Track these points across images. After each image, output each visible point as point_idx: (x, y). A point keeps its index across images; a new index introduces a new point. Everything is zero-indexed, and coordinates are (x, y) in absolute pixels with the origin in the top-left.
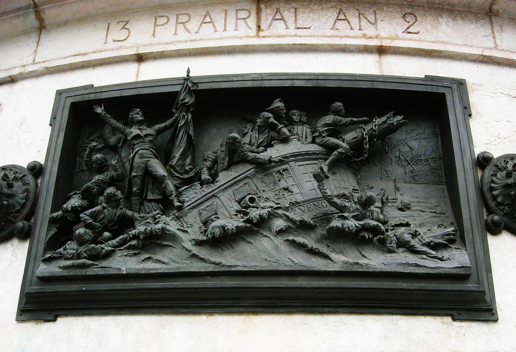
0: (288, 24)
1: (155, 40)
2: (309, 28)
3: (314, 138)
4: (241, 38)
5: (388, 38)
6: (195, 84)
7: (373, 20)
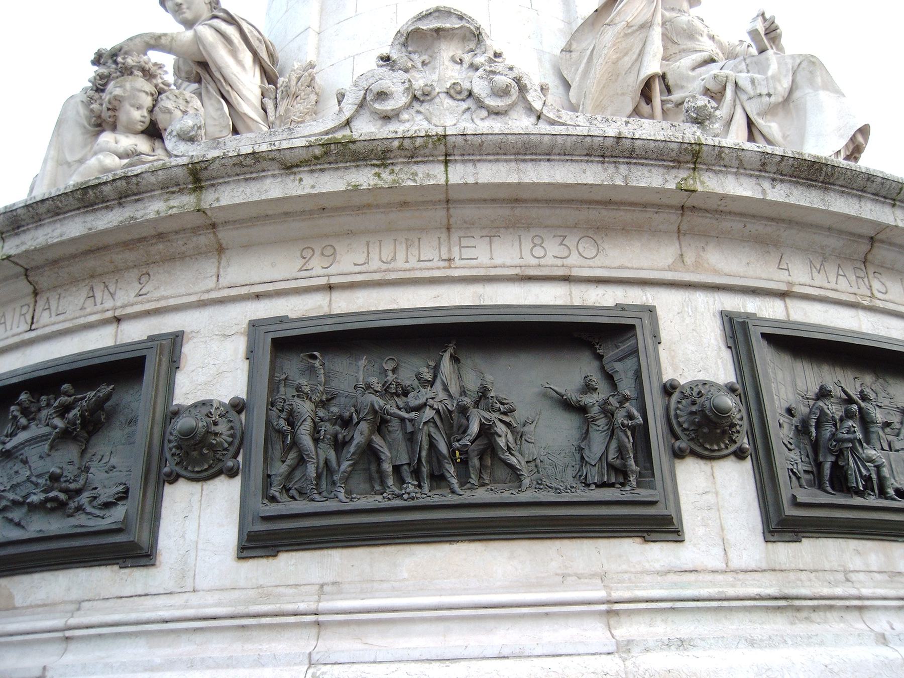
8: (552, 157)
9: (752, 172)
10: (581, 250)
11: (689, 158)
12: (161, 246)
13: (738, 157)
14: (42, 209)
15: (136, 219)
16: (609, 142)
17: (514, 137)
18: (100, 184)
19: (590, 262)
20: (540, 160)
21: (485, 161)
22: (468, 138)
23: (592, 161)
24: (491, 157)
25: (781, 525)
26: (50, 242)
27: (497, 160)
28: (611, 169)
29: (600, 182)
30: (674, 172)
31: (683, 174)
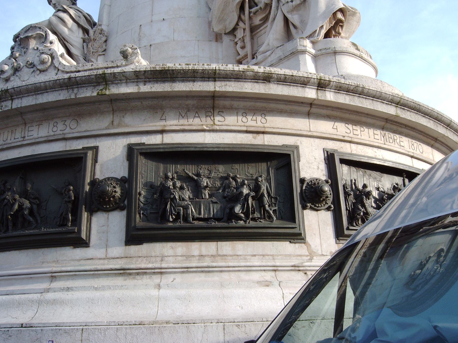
8: (48, 91)
9: (133, 80)
10: (71, 125)
11: (102, 80)
13: (123, 76)
16: (66, 81)
17: (31, 86)
19: (73, 131)
20: (44, 93)
21: (25, 96)
22: (15, 89)
23: (63, 89)
24: (26, 95)
25: (134, 237)
27: (29, 96)
28: (71, 91)
29: (65, 98)
30: (97, 87)
31: (101, 87)
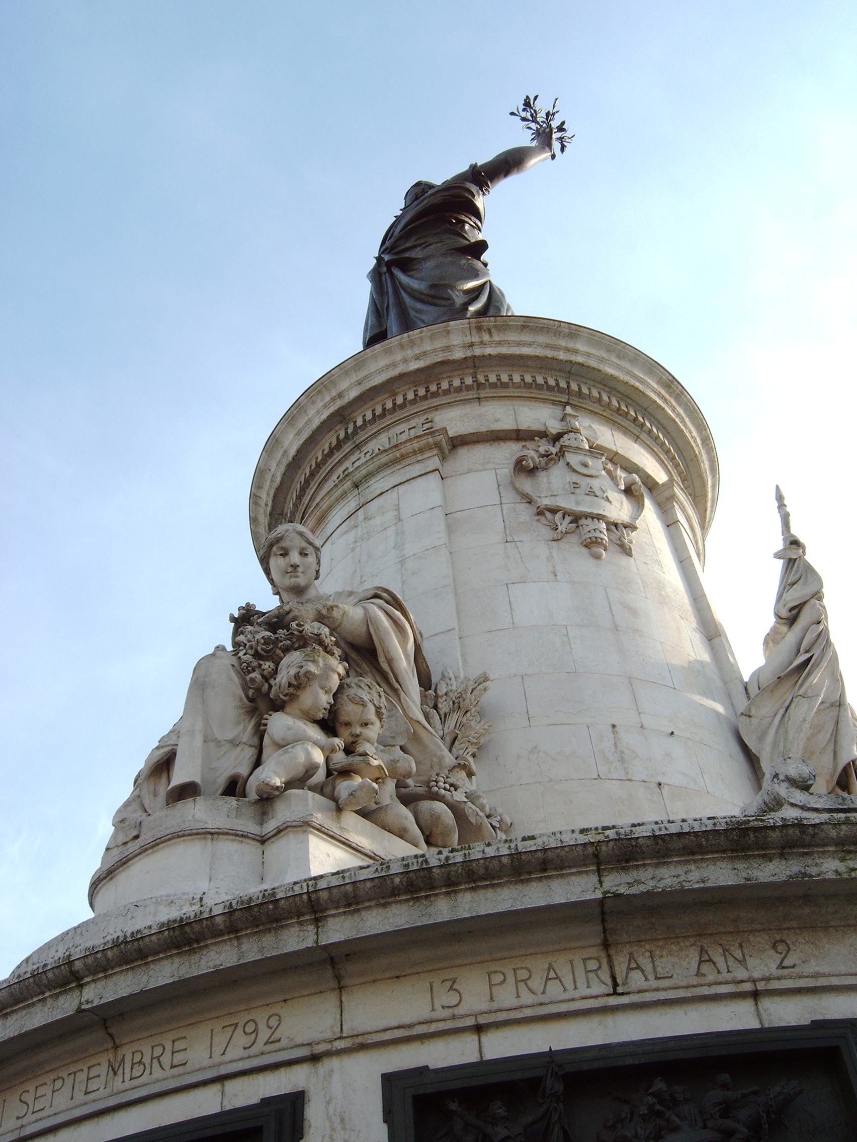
0: (646, 973)
1: (495, 1006)
2: (671, 977)
3: (704, 1121)
4: (596, 997)
5: (763, 979)
6: (560, 1066)
7: (740, 957)
12: (806, 910)
14: (677, 844)
15: (811, 876)
18: (766, 828)
26: (687, 886)
